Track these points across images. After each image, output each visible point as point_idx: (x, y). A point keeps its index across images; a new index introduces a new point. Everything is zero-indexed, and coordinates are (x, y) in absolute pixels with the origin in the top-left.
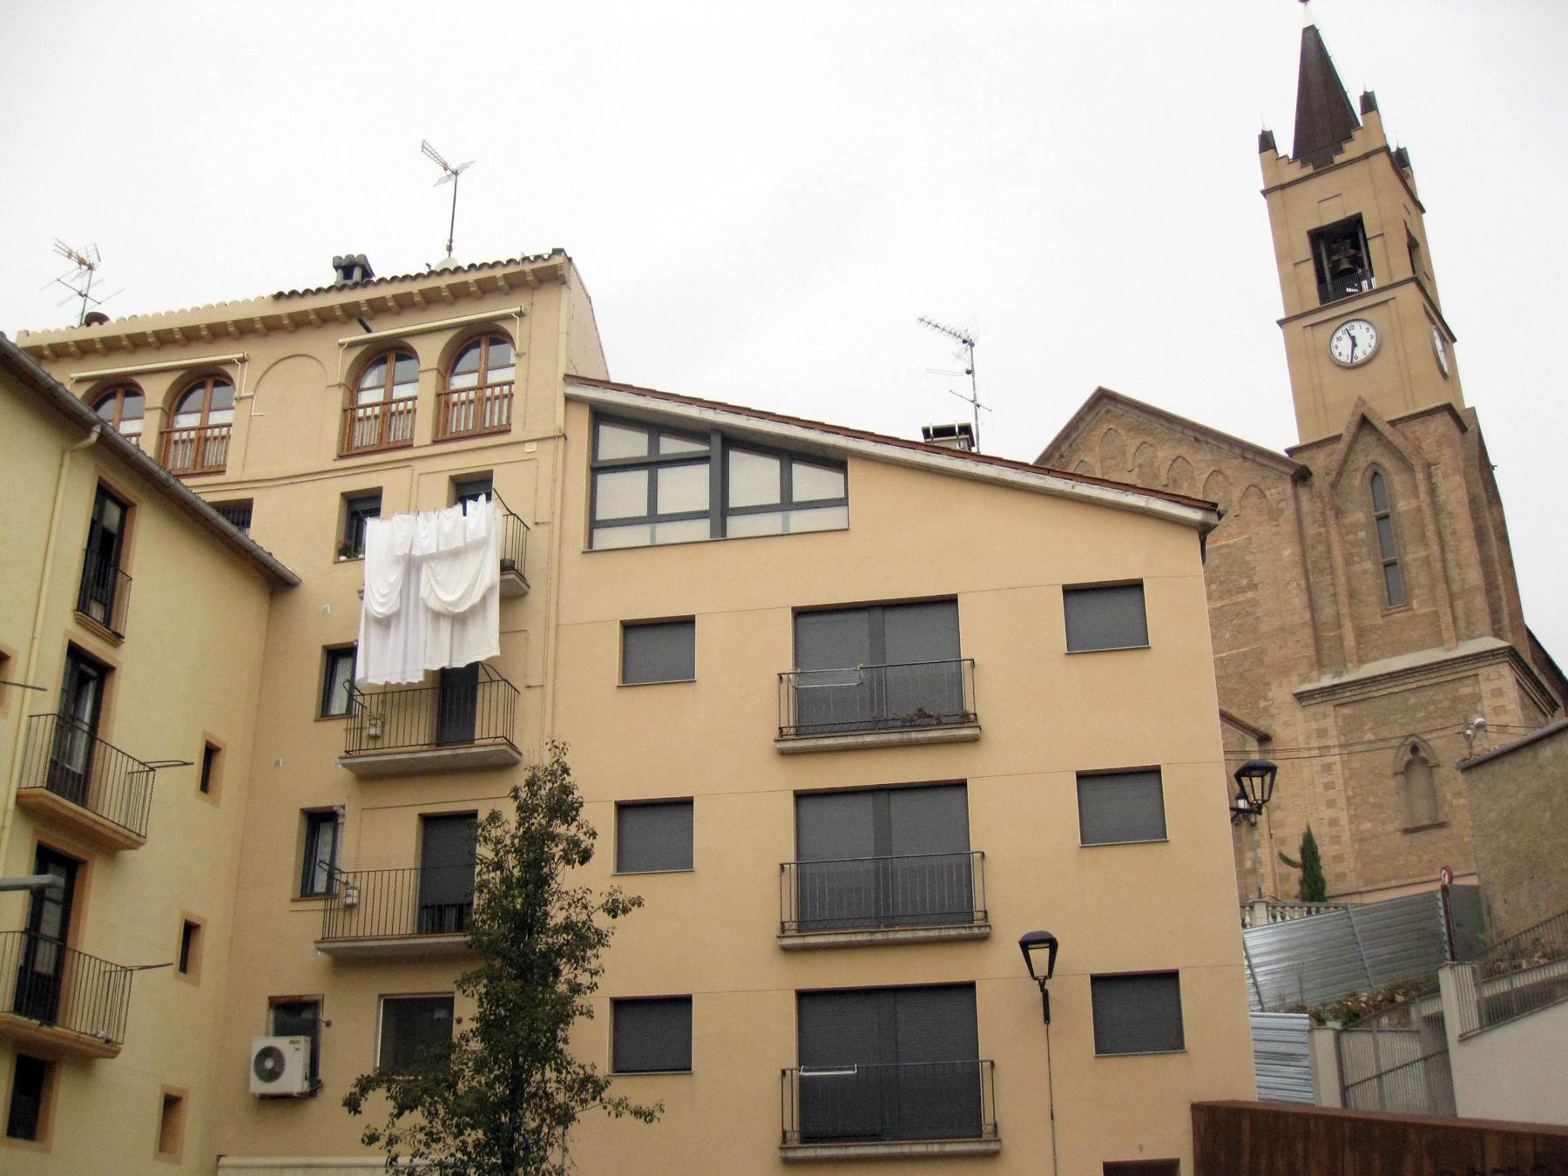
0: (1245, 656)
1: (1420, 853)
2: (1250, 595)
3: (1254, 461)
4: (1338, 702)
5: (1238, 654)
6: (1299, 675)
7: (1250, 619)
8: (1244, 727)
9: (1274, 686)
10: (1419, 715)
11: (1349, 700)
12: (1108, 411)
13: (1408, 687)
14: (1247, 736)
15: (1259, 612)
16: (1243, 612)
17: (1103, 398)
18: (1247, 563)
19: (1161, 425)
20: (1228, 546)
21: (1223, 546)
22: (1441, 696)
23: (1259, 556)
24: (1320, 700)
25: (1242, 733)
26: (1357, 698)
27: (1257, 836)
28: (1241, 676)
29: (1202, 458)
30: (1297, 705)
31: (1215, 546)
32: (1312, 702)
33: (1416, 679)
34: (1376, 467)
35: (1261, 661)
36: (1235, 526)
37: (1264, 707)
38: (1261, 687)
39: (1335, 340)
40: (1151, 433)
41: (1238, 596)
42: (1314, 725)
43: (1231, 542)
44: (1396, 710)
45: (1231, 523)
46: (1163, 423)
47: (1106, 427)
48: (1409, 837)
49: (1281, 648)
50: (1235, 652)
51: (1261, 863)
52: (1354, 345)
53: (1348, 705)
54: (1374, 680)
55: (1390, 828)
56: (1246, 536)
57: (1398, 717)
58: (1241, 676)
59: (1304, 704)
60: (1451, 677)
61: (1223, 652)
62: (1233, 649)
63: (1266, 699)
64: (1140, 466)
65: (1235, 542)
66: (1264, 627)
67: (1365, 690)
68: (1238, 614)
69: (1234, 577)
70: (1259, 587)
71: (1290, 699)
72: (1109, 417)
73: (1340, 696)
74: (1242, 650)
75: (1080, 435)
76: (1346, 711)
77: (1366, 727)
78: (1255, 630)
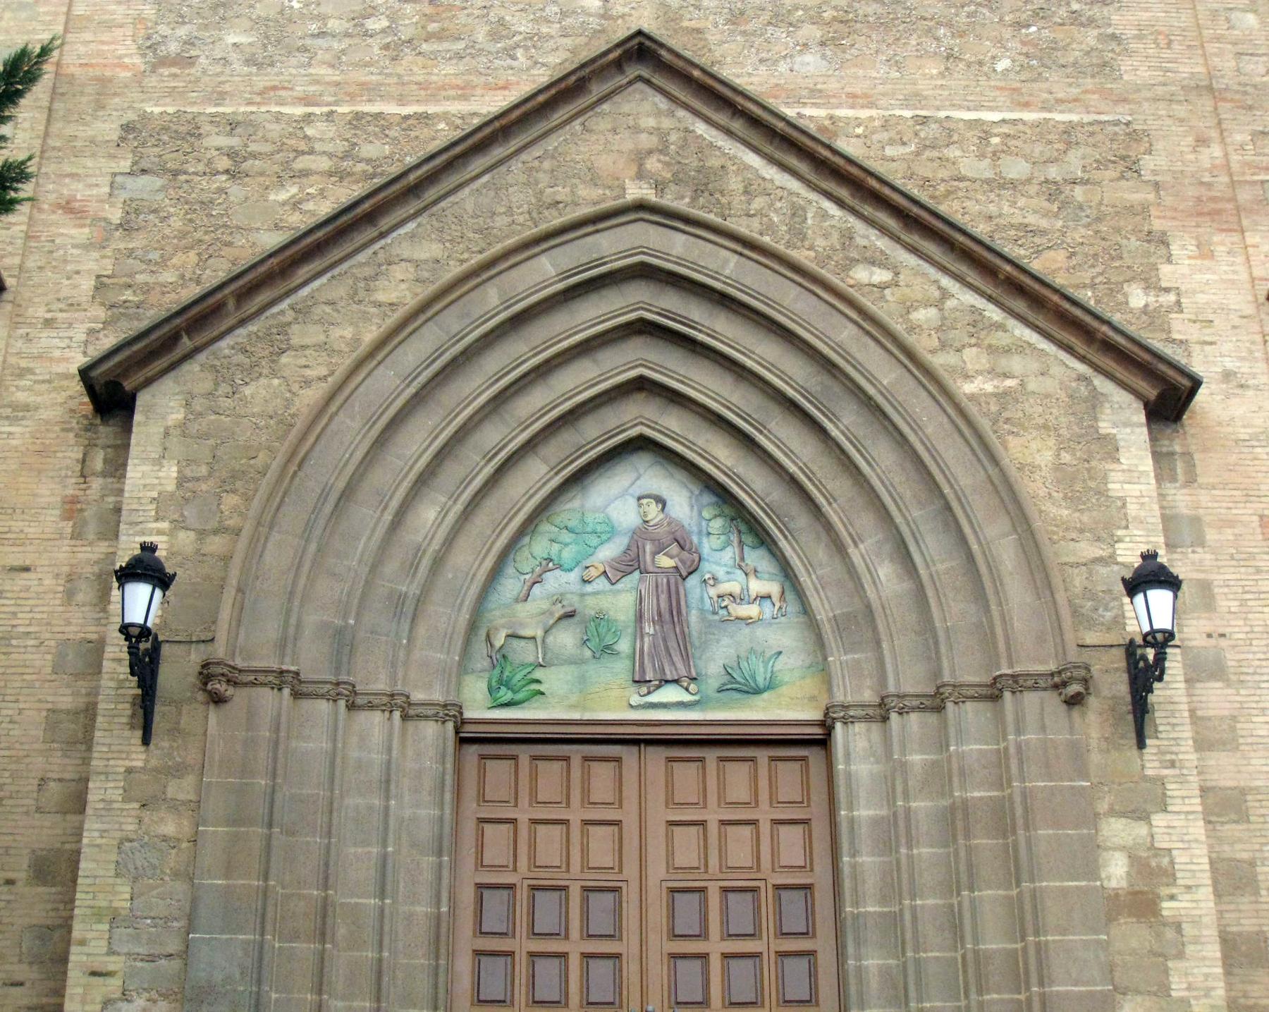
0: (1068, 130)
5: (1037, 124)
7: (1090, 37)
8: (1109, 347)
9: (1182, 248)
14: (1101, 383)
16: (1063, 12)
27: (1151, 762)
28: (1053, 191)
35: (1131, 168)
37: (1145, 310)
49: (1202, 141)
50: (1030, 116)
51: (1170, 875)
58: (1053, 191)
61: (991, 109)
62: (1026, 105)
63: (1151, 284)
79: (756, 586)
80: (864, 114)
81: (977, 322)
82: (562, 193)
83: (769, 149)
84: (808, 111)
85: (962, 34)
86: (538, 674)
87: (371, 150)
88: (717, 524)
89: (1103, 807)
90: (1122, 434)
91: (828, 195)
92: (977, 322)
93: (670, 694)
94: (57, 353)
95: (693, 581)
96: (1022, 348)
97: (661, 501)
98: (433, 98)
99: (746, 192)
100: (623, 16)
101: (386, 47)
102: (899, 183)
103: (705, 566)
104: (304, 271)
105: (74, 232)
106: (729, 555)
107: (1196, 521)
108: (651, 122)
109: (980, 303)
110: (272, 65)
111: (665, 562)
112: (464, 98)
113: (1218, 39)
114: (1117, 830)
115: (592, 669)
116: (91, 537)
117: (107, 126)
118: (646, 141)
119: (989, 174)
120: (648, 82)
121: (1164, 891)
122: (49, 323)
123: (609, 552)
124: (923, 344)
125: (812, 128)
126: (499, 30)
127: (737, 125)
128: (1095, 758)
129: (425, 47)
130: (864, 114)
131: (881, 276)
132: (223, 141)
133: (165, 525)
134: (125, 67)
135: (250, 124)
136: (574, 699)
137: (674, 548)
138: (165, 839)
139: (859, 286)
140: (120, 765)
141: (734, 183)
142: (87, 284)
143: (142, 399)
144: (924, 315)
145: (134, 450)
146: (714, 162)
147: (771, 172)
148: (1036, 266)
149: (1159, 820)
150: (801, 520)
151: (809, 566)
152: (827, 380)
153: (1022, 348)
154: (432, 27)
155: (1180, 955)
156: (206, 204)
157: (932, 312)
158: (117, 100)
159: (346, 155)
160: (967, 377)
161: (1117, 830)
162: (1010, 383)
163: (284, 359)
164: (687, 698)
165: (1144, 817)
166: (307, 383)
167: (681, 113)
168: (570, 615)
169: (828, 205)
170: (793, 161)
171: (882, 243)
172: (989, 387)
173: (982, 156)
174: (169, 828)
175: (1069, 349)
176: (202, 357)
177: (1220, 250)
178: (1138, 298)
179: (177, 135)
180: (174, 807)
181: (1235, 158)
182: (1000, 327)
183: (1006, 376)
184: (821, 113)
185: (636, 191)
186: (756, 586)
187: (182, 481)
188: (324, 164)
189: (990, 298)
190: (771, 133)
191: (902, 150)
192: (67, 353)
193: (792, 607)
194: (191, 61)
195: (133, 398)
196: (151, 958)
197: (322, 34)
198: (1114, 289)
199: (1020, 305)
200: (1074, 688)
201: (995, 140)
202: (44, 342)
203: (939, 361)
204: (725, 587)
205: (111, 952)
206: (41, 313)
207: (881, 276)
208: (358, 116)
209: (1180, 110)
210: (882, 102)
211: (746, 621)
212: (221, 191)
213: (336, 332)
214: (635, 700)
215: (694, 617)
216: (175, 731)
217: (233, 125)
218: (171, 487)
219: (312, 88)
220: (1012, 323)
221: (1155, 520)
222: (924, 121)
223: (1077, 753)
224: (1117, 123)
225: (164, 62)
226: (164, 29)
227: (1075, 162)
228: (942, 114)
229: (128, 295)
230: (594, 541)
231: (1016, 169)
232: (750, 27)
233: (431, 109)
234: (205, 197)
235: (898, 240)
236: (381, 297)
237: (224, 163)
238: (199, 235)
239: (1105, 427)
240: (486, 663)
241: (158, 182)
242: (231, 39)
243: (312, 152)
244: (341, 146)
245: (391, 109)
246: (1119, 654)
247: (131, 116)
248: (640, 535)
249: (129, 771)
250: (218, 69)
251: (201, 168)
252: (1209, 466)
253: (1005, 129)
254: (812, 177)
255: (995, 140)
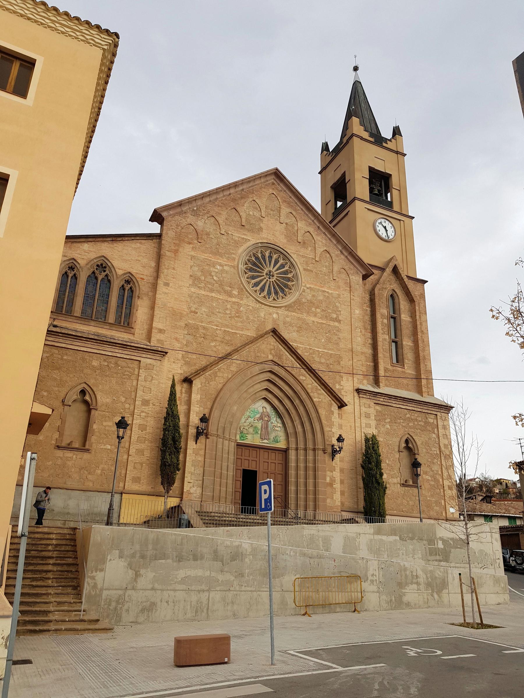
1: (408, 499)
2: (336, 324)
3: (346, 257)
4: (377, 402)
6: (358, 379)
7: (336, 338)
8: (335, 397)
9: (344, 379)
10: (411, 424)
11: (381, 403)
12: (273, 184)
13: (408, 408)
15: (341, 335)
17: (277, 174)
18: (337, 307)
19: (302, 209)
20: (328, 292)
21: (326, 291)
22: (420, 419)
23: (343, 306)
24: (368, 397)
25: (330, 399)
26: (385, 404)
29: (321, 240)
30: (356, 394)
31: (322, 289)
32: (365, 396)
33: (412, 405)
34: (394, 293)
35: (339, 363)
36: (332, 284)
38: (338, 377)
39: (378, 223)
40: (295, 210)
41: (330, 322)
42: (364, 409)
43: (330, 291)
44: (401, 417)
45: (331, 282)
46: (304, 209)
47: (271, 191)
48: (403, 488)
50: (326, 351)
52: (386, 231)
53: (380, 405)
54: (396, 398)
55: (395, 480)
56: (338, 293)
57: (402, 421)
59: (360, 396)
60: (426, 411)
62: (325, 349)
64: (286, 224)
65: (332, 293)
66: (342, 345)
67: (390, 401)
68: (329, 331)
69: (329, 311)
70: (342, 322)
71: (351, 389)
72: (273, 187)
73: (378, 399)
74: (330, 352)
75: (255, 185)
76: (378, 408)
77: (386, 421)
78: (337, 344)
79: (279, 425)
80: (302, 346)
81: (317, 389)
82: (259, 354)
83: (290, 353)
84: (294, 344)
85: (317, 333)
86: (247, 435)
87: (227, 338)
88: (274, 413)
89: (327, 470)
90: (334, 411)
91: (298, 363)
92: (317, 389)
93: (266, 441)
94: (176, 369)
95: (269, 423)
96: (323, 394)
97: (266, 408)
98: (237, 330)
99: (286, 359)
100: (267, 319)
101: (229, 317)
102: (306, 360)
103: (272, 420)
104: (220, 362)
105: (178, 344)
106: (275, 419)
107: (341, 425)
108: (273, 344)
109: (317, 385)
110: (210, 317)
111: (266, 419)
112: (242, 331)
113: (354, 342)
114: (328, 473)
115: (254, 435)
116: (183, 405)
117: (182, 323)
118: (272, 347)
119: (319, 361)
120: (273, 336)
121: (334, 483)
122: (174, 362)
123: (258, 416)
124: (309, 391)
125: (294, 347)
126: (248, 318)
127: (286, 347)
128: (327, 462)
129: (236, 319)
130: (302, 346)
131: (304, 378)
132: (203, 331)
133: (198, 406)
134: (185, 311)
135: (207, 328)
136: (252, 440)
137: (267, 417)
138: (199, 461)
139: (301, 379)
140: (192, 447)
141: (284, 358)
142: (181, 356)
143: (194, 382)
144: (309, 386)
145: (193, 391)
146: (282, 353)
147: (290, 357)
148: (324, 378)
149: (334, 472)
150: (287, 416)
151: (287, 423)
152: (295, 395)
153: (323, 394)
154: (237, 315)
155: (335, 493)
156: (200, 343)
157: (311, 386)
158: (184, 318)
159: (223, 338)
160: (315, 398)
161: (328, 473)
162: (320, 400)
163: (217, 378)
164: (268, 442)
165: (332, 472)
166: (220, 383)
167: (277, 343)
168: (252, 426)
169: (297, 364)
170: (294, 356)
171: (305, 372)
172: (317, 400)
173: (318, 357)
174: (200, 459)
175: (329, 396)
176: (203, 376)
177: (350, 380)
178: (338, 387)
179: (194, 328)
180: (201, 455)
181: (354, 364)
182: (320, 390)
183: (320, 398)
184: (296, 345)
185: (270, 357)
186: (279, 425)
187: (201, 398)
188: (220, 339)
189: (319, 385)
190: (291, 351)
191: (307, 354)
192: (177, 369)
193: (283, 429)
194: (197, 313)
195: (192, 381)
196: (197, 480)
197: (219, 312)
198: (334, 385)
199: (323, 387)
200: (326, 452)
201: (320, 355)
202: (173, 366)
203: (311, 394)
204: (274, 424)
205: (191, 479)
206: (173, 360)
207: (304, 378)
208: (225, 331)
209: (347, 354)
210: (305, 344)
211: (277, 430)
212: (202, 341)
213: (225, 375)
214: (261, 442)
215: (269, 429)
216: (200, 442)
217: (204, 328)
218: (199, 399)
219: (217, 323)
220: (321, 389)
221: (338, 425)
222: (310, 349)
223: (325, 461)
224: (338, 354)
225: (191, 312)
226: (192, 305)
227: (331, 361)
228: (313, 348)
229: (187, 359)
230: (256, 414)
231: (323, 361)
232: (286, 326)
233: (237, 332)
234: (200, 342)
235: (307, 373)
236: (231, 369)
237: (202, 335)
238: (199, 349)
239: (332, 409)
240: (239, 433)
241: (192, 337)
242: (203, 310)
243: (217, 336)
244: (222, 336)
245: (230, 330)
246: (331, 446)
247: (186, 322)
248: (262, 414)
249: (193, 448)
250: (201, 316)
251: (199, 336)
252: (344, 416)
253: (322, 353)
254: (296, 359)
255: (320, 355)
